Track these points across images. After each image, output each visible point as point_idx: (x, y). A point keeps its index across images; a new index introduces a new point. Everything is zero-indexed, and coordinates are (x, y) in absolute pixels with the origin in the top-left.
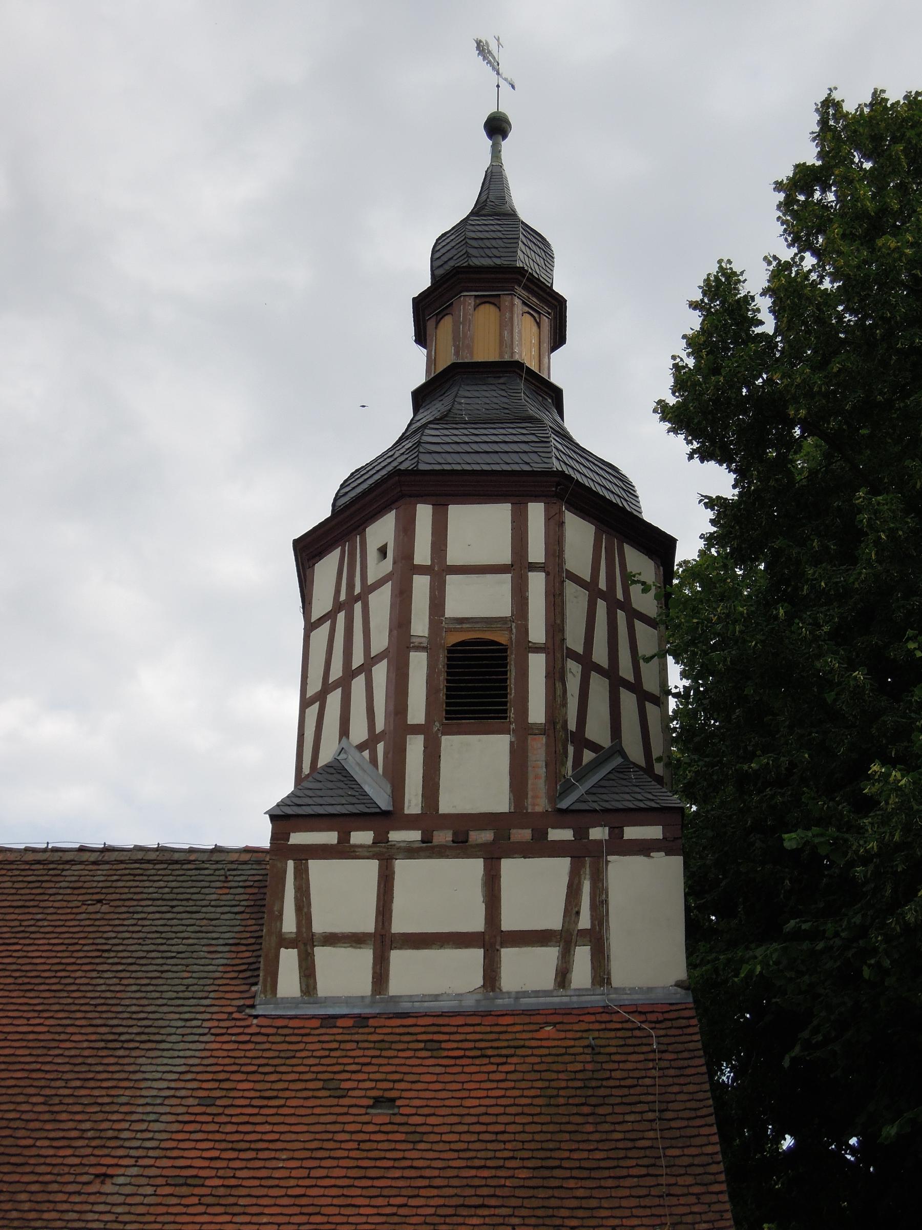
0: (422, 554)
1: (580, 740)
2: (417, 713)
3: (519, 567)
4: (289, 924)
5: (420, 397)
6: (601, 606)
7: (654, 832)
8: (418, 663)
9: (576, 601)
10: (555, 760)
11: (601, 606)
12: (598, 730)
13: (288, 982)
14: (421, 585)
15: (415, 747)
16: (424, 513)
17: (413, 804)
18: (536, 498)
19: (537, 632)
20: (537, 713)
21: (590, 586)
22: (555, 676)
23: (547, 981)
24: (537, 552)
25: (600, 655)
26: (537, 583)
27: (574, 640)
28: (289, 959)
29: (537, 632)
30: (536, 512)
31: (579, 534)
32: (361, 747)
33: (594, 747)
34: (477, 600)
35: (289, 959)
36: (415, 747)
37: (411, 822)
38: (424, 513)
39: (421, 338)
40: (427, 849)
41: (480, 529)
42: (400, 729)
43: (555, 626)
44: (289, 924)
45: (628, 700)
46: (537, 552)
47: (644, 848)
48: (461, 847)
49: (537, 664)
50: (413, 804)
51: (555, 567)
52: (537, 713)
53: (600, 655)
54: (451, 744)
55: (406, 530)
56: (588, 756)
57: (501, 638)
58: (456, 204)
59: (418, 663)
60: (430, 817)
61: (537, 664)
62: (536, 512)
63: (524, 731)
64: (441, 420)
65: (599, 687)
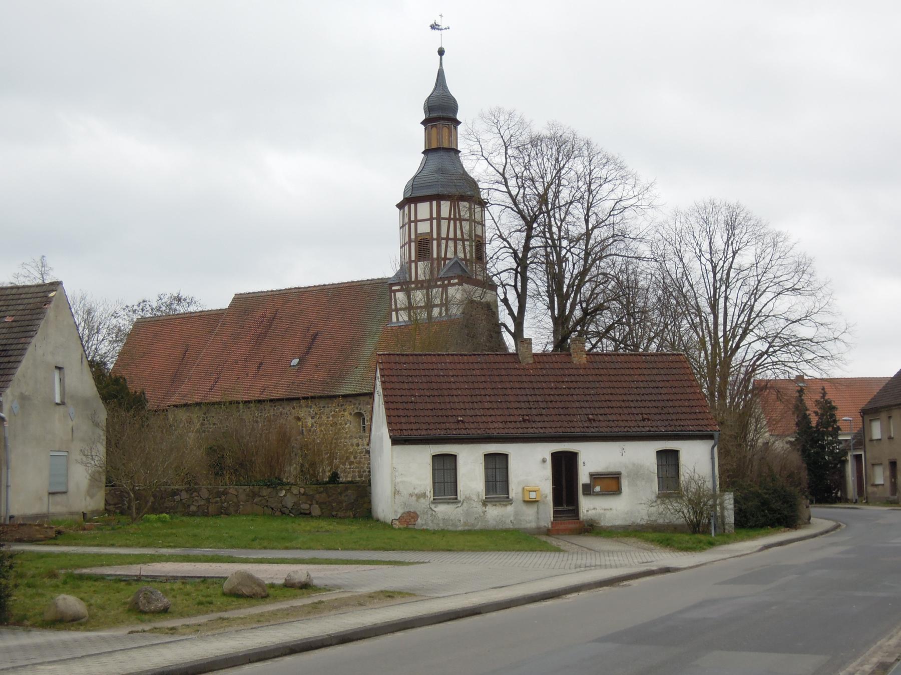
0: (413, 218)
1: (445, 259)
2: (413, 258)
3: (431, 219)
4: (393, 307)
7: (456, 281)
8: (413, 244)
9: (444, 224)
10: (439, 264)
12: (450, 255)
13: (394, 319)
14: (413, 225)
15: (413, 265)
16: (413, 206)
17: (413, 279)
18: (434, 200)
19: (435, 236)
20: (435, 256)
22: (439, 246)
24: (435, 215)
26: (435, 222)
27: (444, 235)
28: (394, 313)
29: (435, 236)
30: (434, 203)
31: (445, 206)
33: (449, 259)
34: (424, 228)
35: (394, 313)
36: (413, 265)
37: (413, 283)
38: (413, 206)
40: (417, 288)
42: (411, 261)
43: (439, 233)
44: (393, 307)
45: (460, 243)
46: (435, 215)
47: (454, 285)
48: (422, 288)
49: (435, 242)
50: (413, 279)
51: (439, 218)
52: (435, 256)
54: (419, 263)
58: (428, 88)
59: (413, 244)
60: (417, 281)
61: (435, 242)
63: (433, 259)
65: (451, 244)
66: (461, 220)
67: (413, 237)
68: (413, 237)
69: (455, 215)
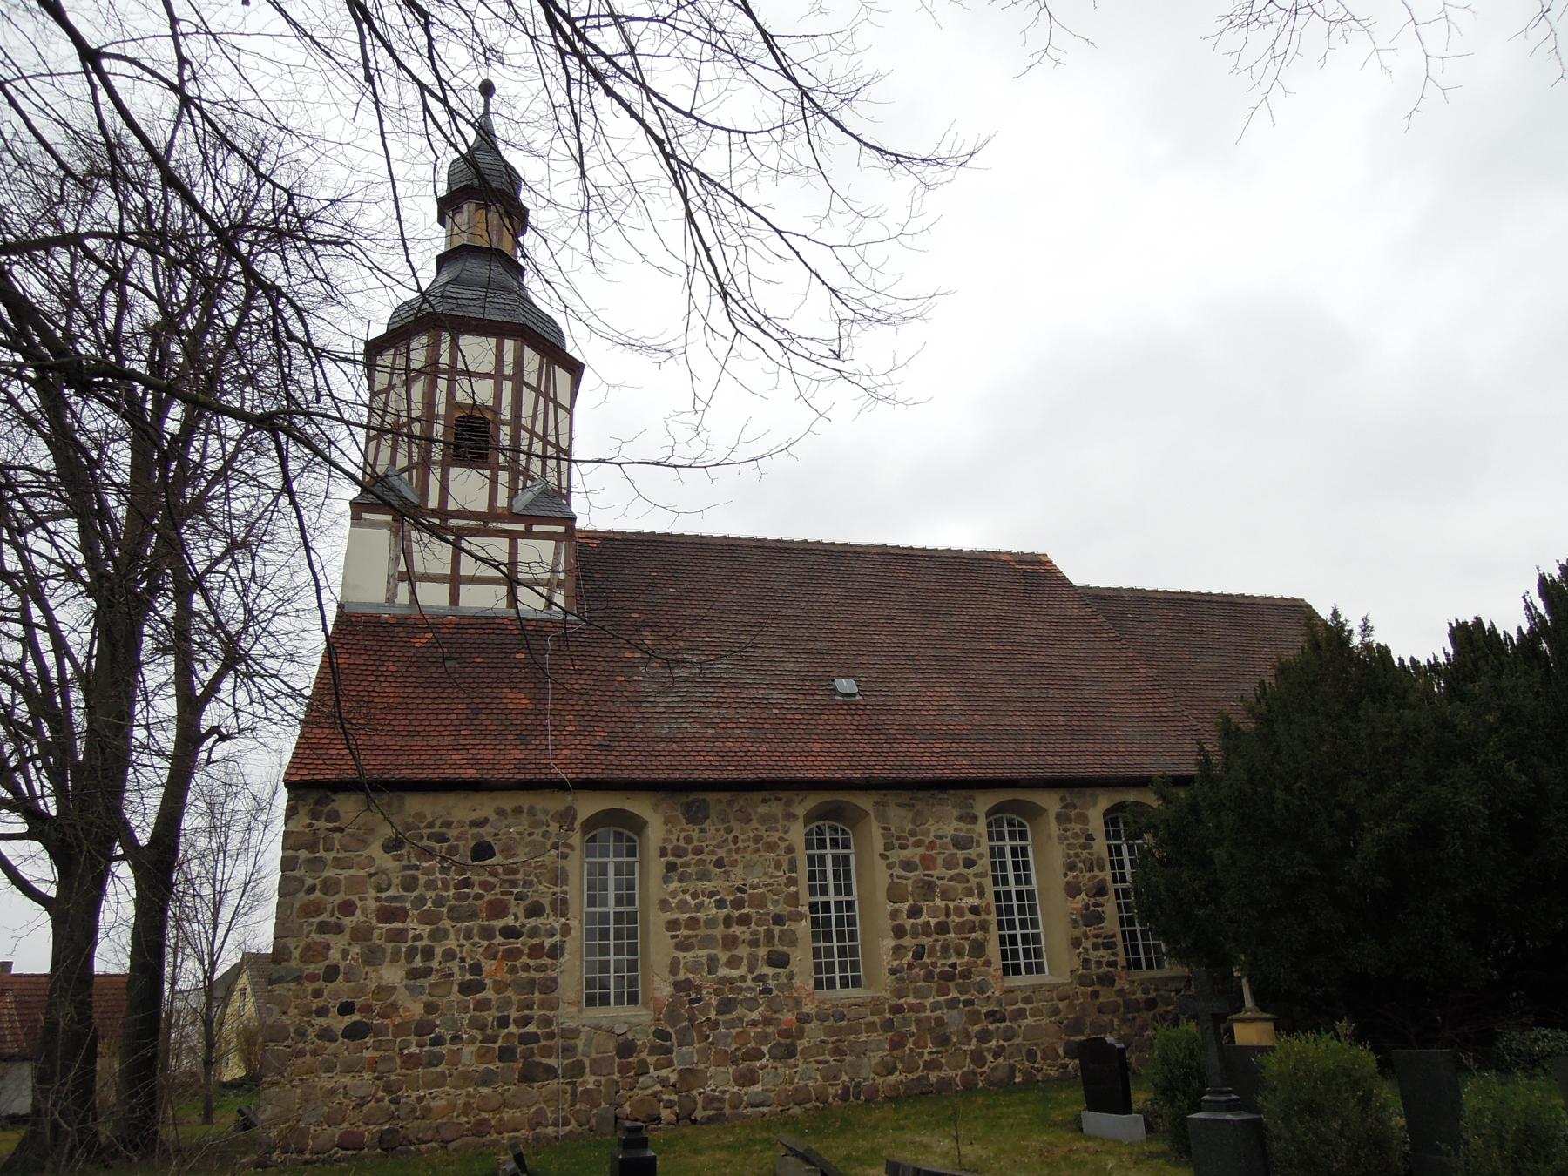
3: (497, 376)
5: (442, 260)
6: (541, 400)
9: (528, 397)
11: (541, 400)
15: (437, 471)
18: (509, 336)
19: (506, 412)
21: (536, 390)
23: (503, 604)
24: (508, 370)
25: (539, 429)
26: (508, 386)
29: (506, 412)
31: (532, 359)
32: (403, 470)
33: (533, 479)
38: (446, 337)
39: (442, 221)
41: (477, 351)
46: (508, 370)
49: (506, 429)
50: (433, 503)
53: (539, 429)
55: (434, 347)
56: (529, 483)
57: (489, 416)
60: (443, 512)
62: (509, 344)
64: (453, 281)
66: (557, 405)
67: (441, 409)
68: (441, 409)
69: (547, 388)
